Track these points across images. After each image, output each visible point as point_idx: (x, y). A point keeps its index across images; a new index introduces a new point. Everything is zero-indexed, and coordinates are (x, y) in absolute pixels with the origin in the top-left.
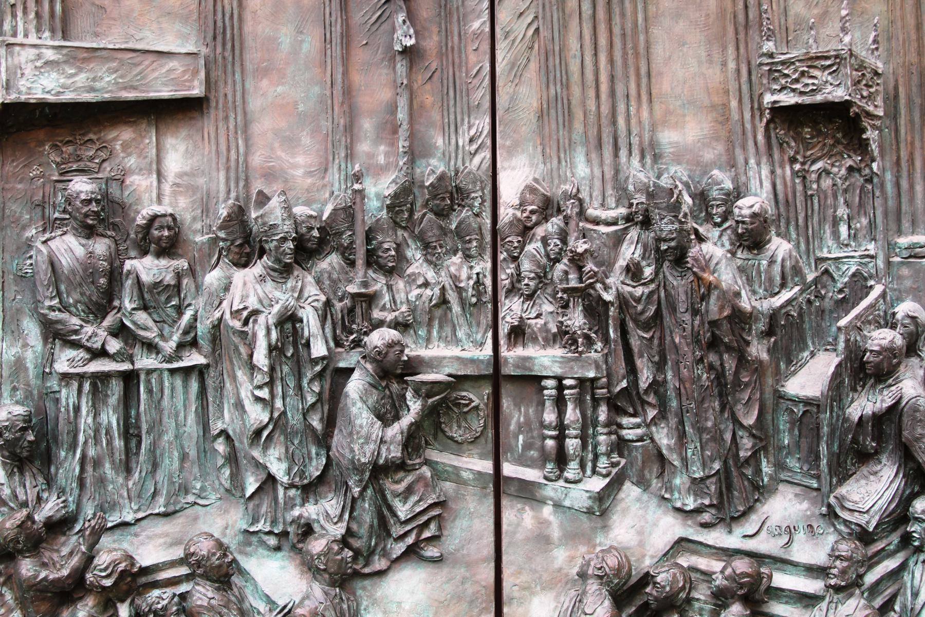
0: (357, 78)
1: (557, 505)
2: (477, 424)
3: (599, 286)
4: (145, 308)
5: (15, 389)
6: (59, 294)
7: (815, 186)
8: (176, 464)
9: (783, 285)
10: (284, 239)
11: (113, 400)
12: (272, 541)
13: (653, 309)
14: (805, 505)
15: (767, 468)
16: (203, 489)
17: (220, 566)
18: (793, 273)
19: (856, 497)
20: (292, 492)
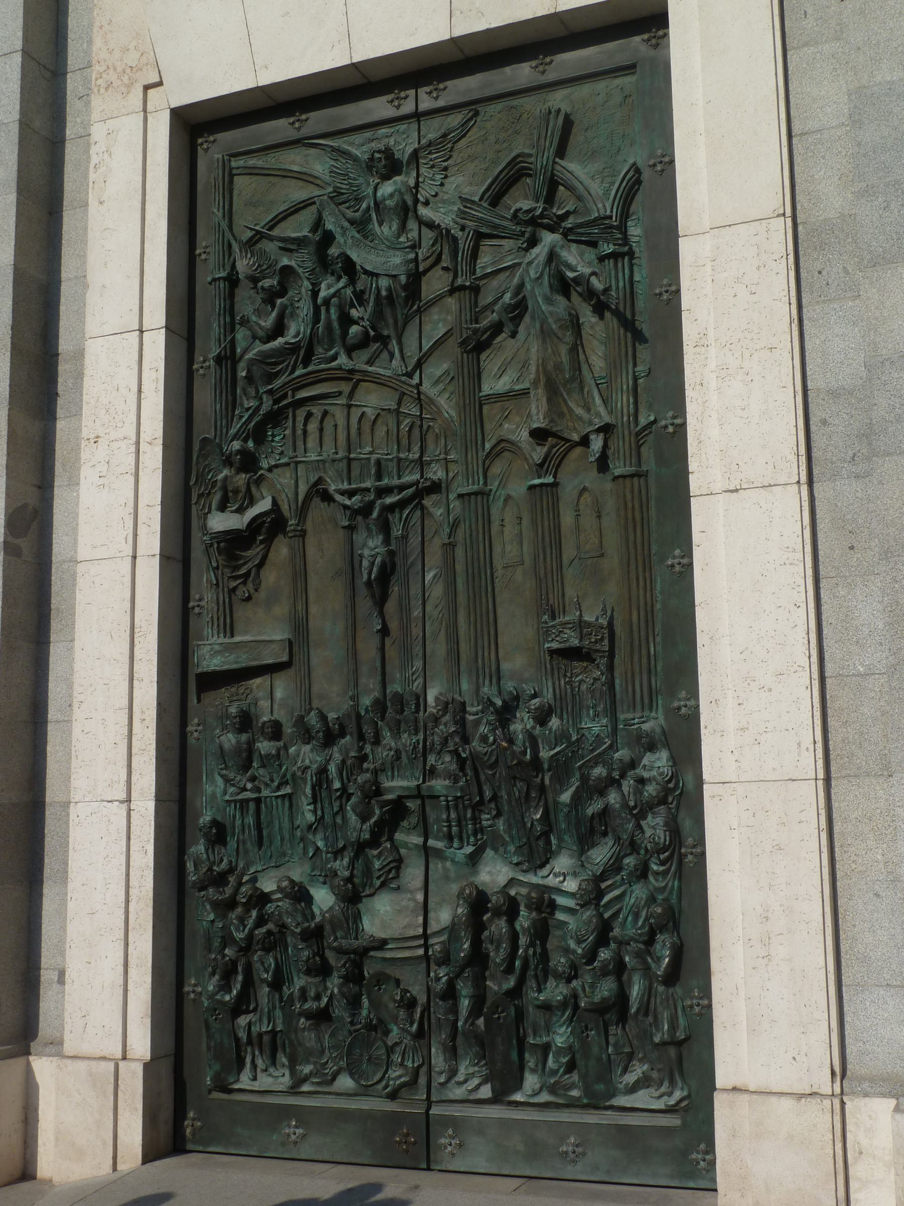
0: (360, 645)
1: (453, 861)
2: (414, 820)
3: (460, 749)
4: (263, 766)
5: (212, 807)
6: (225, 762)
7: (577, 689)
8: (279, 843)
9: (556, 745)
10: (318, 732)
11: (251, 812)
12: (321, 879)
13: (494, 758)
14: (573, 861)
15: (554, 841)
16: (292, 854)
17: (291, 892)
18: (562, 736)
19: (594, 857)
20: (329, 855)
